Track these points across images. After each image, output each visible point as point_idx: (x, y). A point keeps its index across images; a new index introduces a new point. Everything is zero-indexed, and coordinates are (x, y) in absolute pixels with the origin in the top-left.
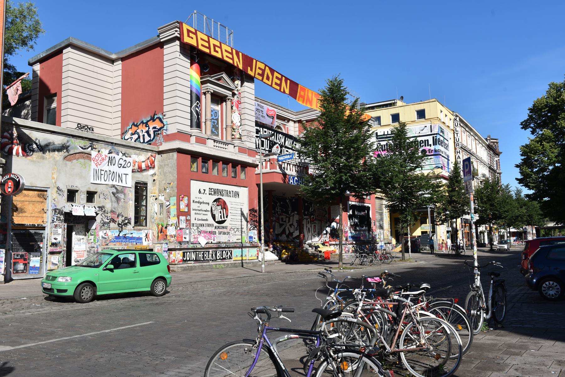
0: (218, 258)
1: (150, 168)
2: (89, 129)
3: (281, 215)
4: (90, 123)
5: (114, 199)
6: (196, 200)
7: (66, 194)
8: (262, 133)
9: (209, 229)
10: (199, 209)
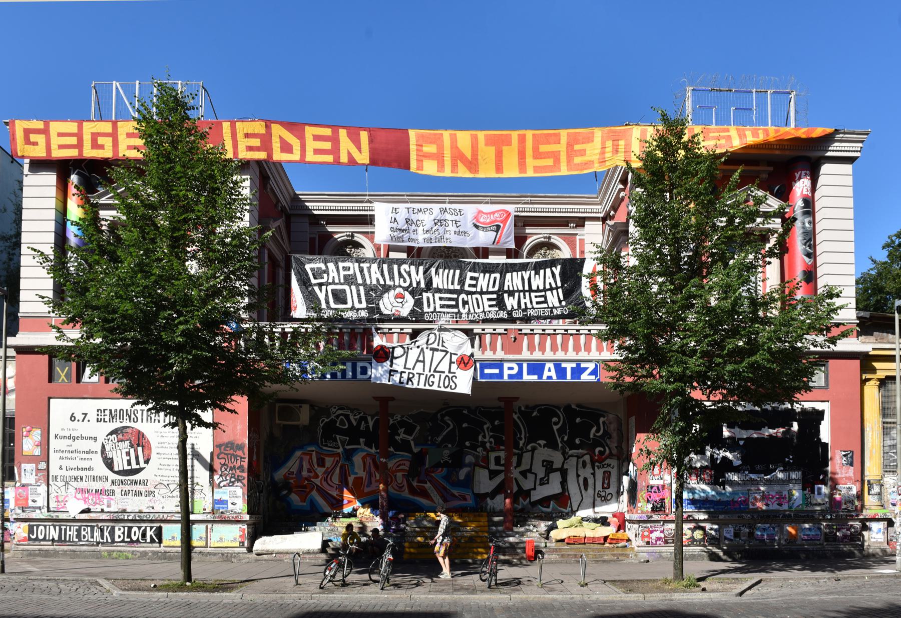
0: (117, 539)
3: (493, 450)
6: (62, 434)
9: (98, 485)
10: (71, 449)
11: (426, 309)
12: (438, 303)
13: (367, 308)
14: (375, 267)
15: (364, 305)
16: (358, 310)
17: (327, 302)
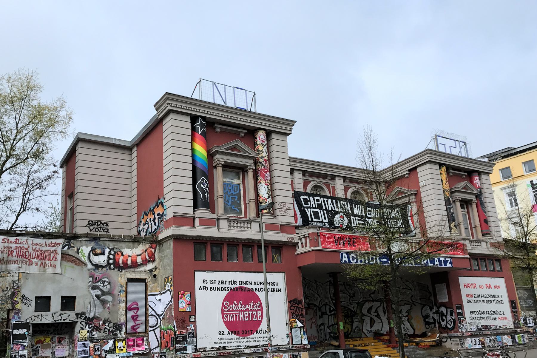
1: (149, 261)
2: (103, 224)
4: (103, 219)
5: (97, 302)
7: (33, 303)
8: (312, 203)
11: (353, 225)
12: (358, 222)
13: (329, 222)
14: (330, 200)
15: (327, 221)
16: (324, 223)
17: (311, 218)
